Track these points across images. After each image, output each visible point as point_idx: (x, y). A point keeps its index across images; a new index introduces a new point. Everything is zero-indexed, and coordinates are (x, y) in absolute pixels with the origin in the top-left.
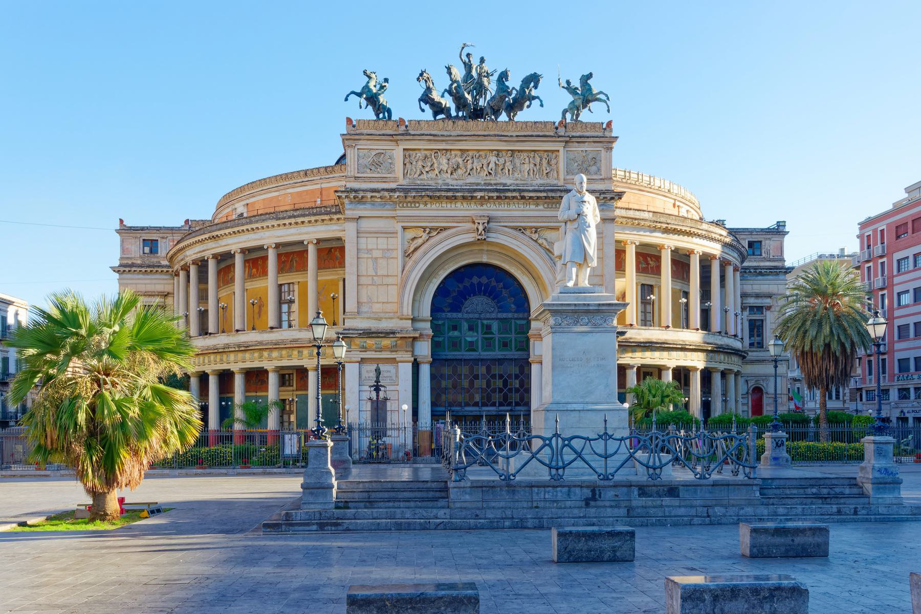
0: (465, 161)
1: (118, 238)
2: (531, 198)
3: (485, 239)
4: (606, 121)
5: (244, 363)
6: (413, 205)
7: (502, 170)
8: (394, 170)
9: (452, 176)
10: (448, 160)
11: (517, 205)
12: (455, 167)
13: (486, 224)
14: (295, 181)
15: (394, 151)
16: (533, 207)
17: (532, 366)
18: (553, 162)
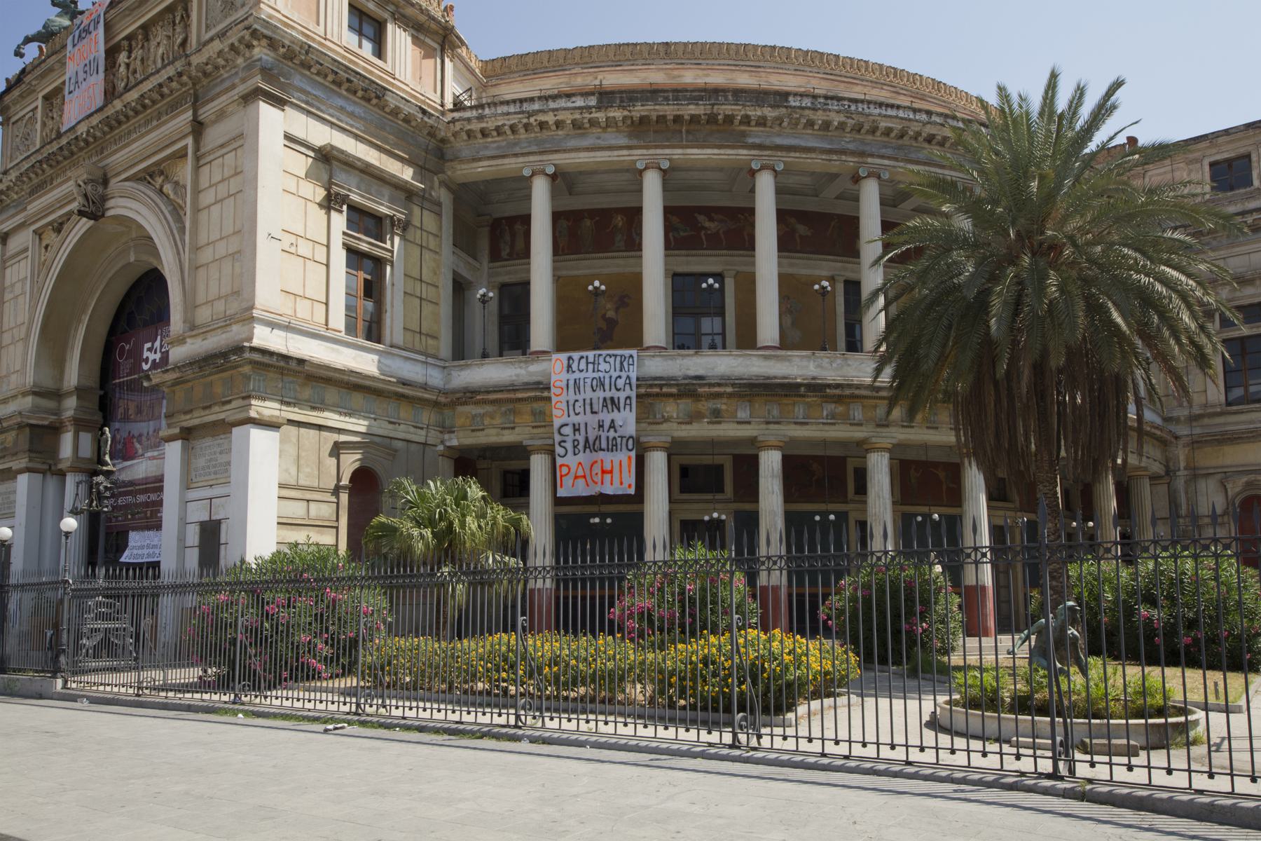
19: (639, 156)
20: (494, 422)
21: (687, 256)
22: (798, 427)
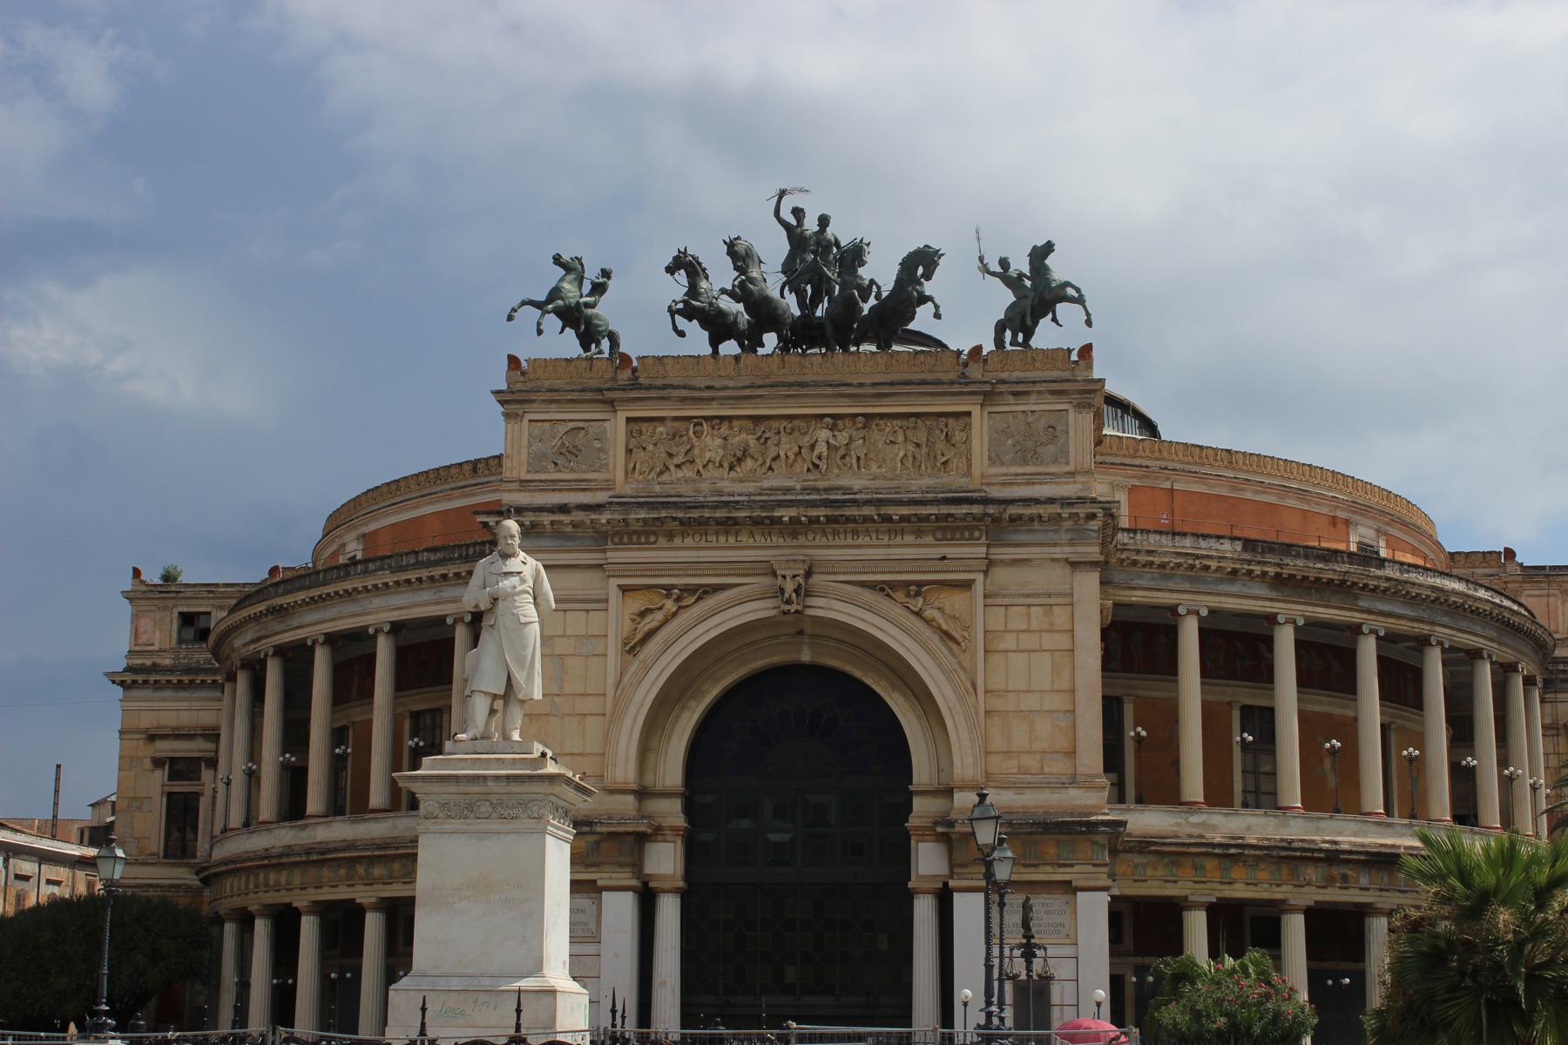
0: (762, 440)
1: (126, 608)
2: (903, 519)
3: (797, 612)
4: (1076, 346)
5: (319, 891)
6: (643, 540)
7: (843, 457)
8: (607, 465)
9: (733, 474)
10: (725, 439)
11: (874, 537)
12: (739, 454)
13: (801, 581)
14: (453, 485)
15: (607, 424)
16: (909, 539)
17: (915, 900)
18: (958, 436)
19: (1282, 609)
20: (1157, 874)
21: (1255, 688)
22: (1401, 895)
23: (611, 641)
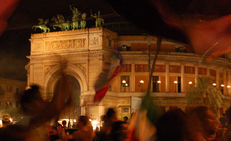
2: (77, 54)
18: (85, 42)
23: (43, 73)
